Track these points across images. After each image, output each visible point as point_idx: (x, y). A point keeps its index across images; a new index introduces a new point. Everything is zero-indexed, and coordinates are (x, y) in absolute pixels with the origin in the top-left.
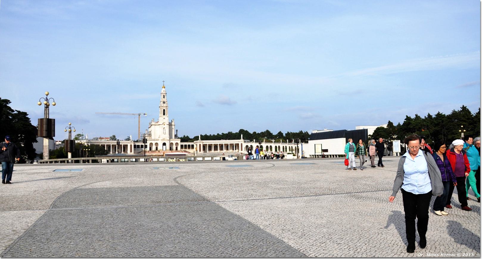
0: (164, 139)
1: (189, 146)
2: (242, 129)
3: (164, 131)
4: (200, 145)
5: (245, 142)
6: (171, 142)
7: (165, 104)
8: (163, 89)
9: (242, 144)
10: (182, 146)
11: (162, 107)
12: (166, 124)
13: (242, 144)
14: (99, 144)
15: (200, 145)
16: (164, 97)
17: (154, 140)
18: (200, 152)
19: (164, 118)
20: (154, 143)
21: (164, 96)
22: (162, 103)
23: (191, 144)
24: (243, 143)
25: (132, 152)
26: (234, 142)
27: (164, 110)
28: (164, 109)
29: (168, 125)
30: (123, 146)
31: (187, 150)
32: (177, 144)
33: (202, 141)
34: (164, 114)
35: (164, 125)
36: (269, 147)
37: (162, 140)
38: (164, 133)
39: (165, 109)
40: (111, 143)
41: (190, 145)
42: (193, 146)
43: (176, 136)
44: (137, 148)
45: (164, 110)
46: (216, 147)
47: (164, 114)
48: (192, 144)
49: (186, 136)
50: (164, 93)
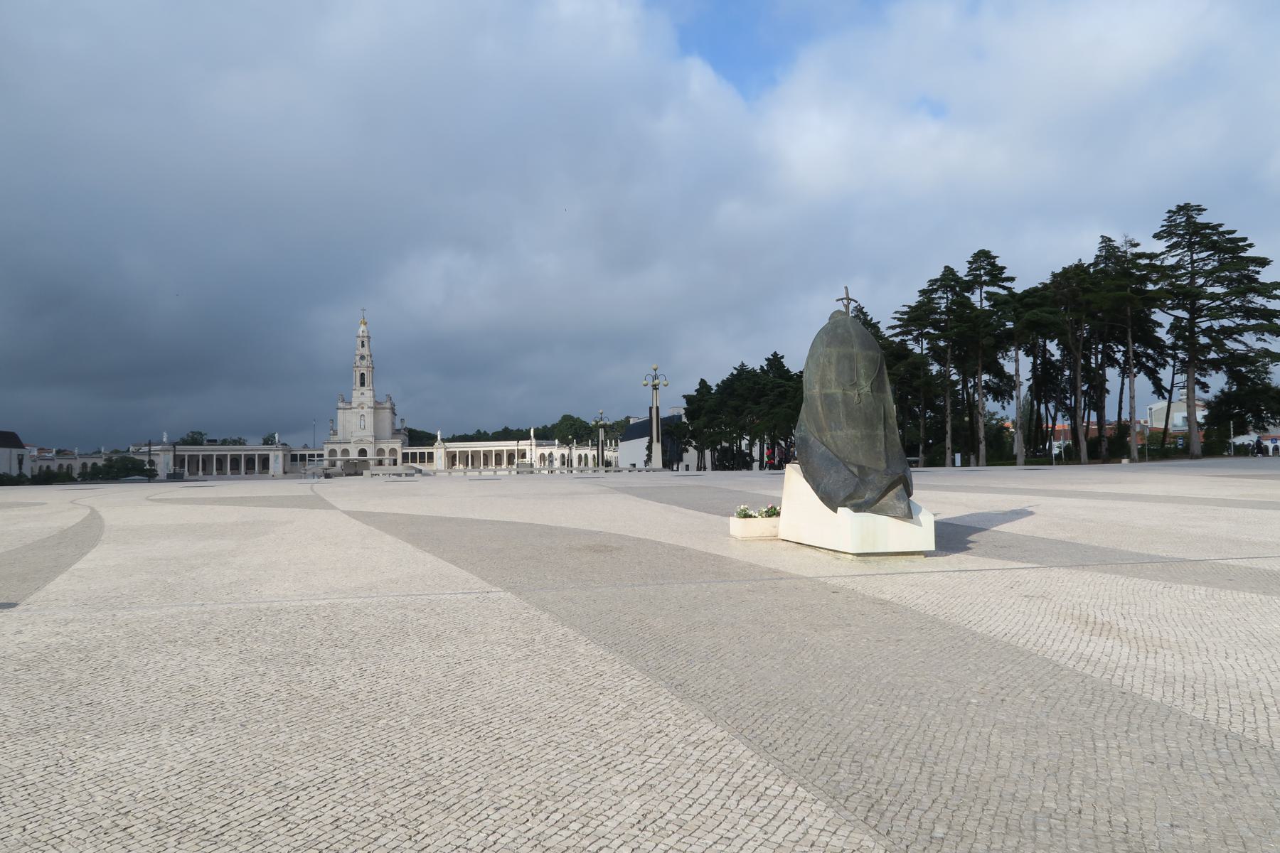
0: (361, 441)
1: (422, 455)
2: (568, 414)
3: (362, 421)
5: (537, 445)
6: (377, 448)
7: (365, 361)
8: (363, 327)
10: (405, 456)
11: (358, 367)
12: (366, 407)
14: (182, 453)
16: (363, 346)
17: (338, 443)
19: (362, 394)
20: (338, 448)
21: (363, 342)
22: (358, 358)
23: (426, 450)
26: (510, 445)
27: (362, 375)
28: (362, 372)
29: (372, 408)
30: (203, 459)
31: (417, 465)
32: (393, 451)
33: (446, 444)
34: (362, 384)
35: (363, 408)
36: (583, 456)
37: (355, 442)
40: (229, 451)
42: (431, 456)
43: (396, 433)
45: (362, 375)
46: (498, 457)
49: (482, 432)
50: (363, 337)
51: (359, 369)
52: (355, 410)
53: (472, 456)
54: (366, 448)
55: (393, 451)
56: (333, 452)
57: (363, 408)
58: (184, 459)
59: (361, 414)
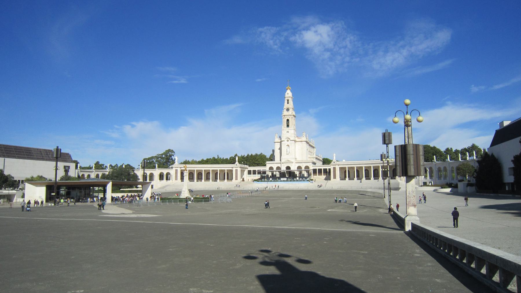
0: (289, 162)
3: (288, 150)
15: (334, 168)
19: (288, 132)
25: (237, 180)
27: (288, 120)
28: (287, 118)
34: (288, 126)
35: (288, 141)
38: (288, 153)
39: (288, 118)
41: (316, 169)
45: (288, 120)
47: (288, 126)
48: (329, 168)
53: (357, 170)
55: (307, 167)
56: (271, 168)
57: (288, 141)
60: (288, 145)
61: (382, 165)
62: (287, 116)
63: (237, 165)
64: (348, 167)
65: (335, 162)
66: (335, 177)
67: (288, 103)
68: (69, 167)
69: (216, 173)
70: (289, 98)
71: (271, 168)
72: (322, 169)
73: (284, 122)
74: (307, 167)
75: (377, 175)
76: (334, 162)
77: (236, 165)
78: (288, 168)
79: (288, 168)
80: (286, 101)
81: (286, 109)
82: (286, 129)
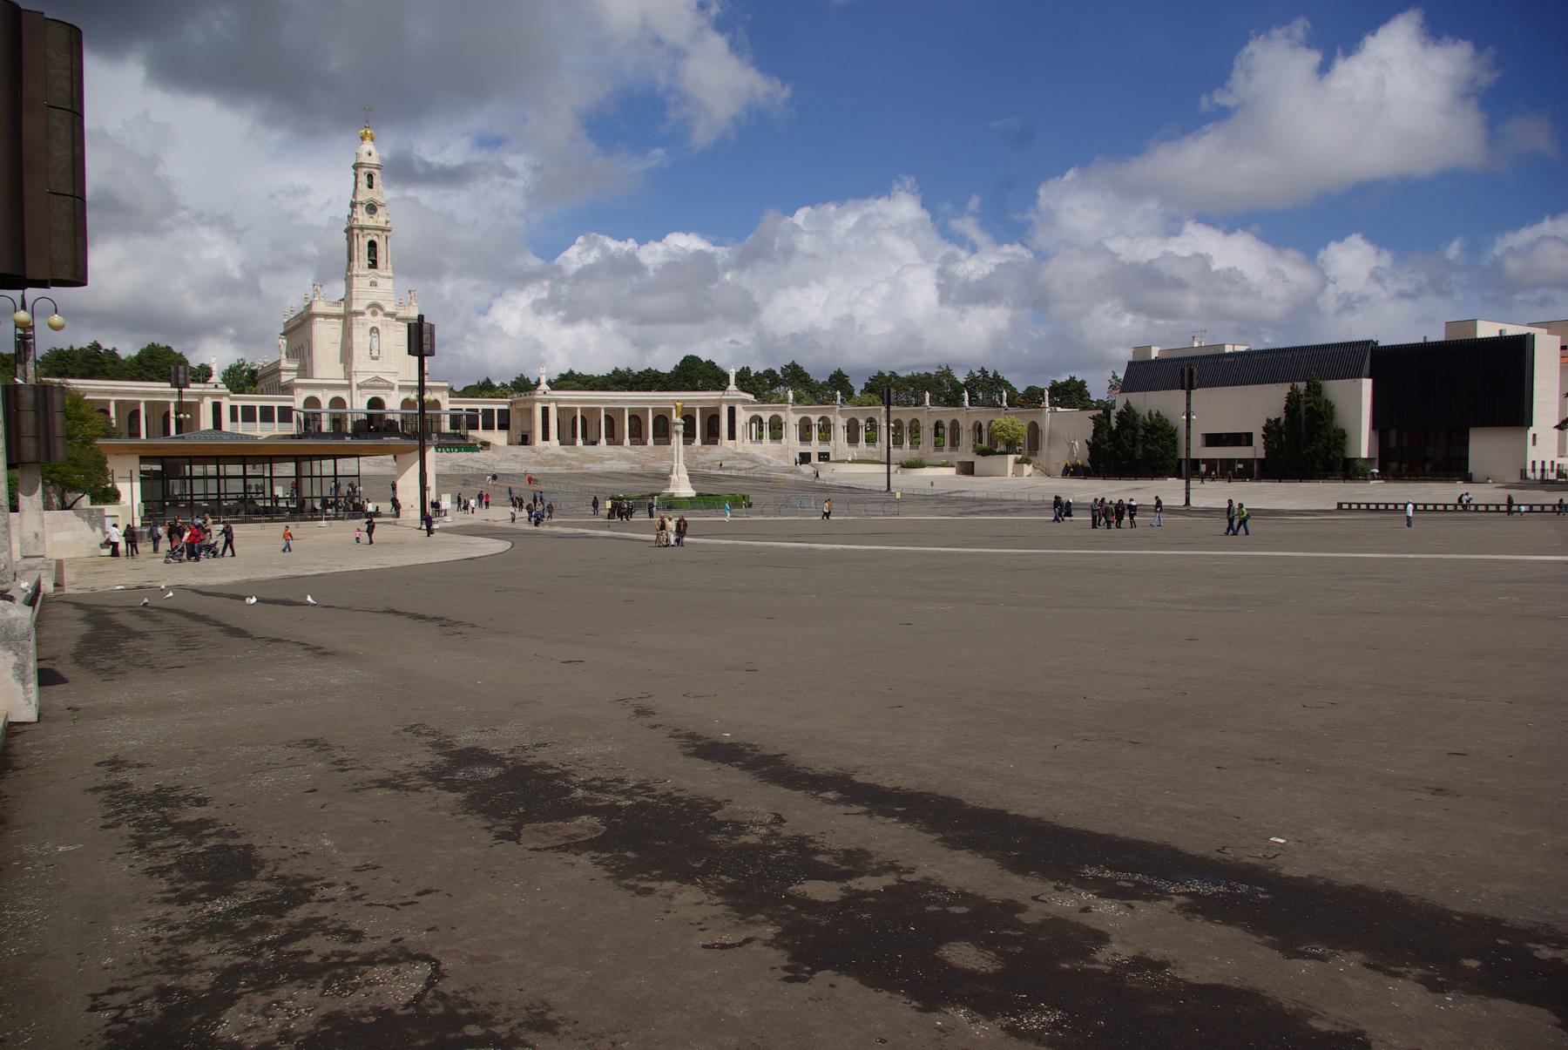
1: (488, 414)
4: (545, 411)
9: (732, 411)
13: (732, 411)
15: (545, 411)
18: (546, 443)
19: (373, 284)
24: (739, 407)
27: (372, 245)
28: (369, 238)
34: (374, 264)
35: (374, 314)
38: (375, 353)
39: (375, 238)
44: (243, 421)
45: (372, 245)
47: (374, 264)
51: (366, 232)
52: (359, 317)
54: (383, 397)
56: (312, 402)
57: (374, 314)
58: (137, 412)
59: (371, 325)
60: (374, 330)
61: (184, 390)
62: (369, 231)
63: (220, 386)
64: (582, 409)
65: (548, 393)
66: (546, 437)
67: (370, 187)
68: (358, 385)
69: (132, 412)
70: (376, 171)
71: (312, 402)
72: (255, 407)
73: (361, 248)
74: (338, 402)
75: (1244, 437)
76: (545, 393)
77: (213, 386)
78: (376, 403)
79: (376, 403)
80: (363, 179)
81: (365, 206)
82: (366, 273)
